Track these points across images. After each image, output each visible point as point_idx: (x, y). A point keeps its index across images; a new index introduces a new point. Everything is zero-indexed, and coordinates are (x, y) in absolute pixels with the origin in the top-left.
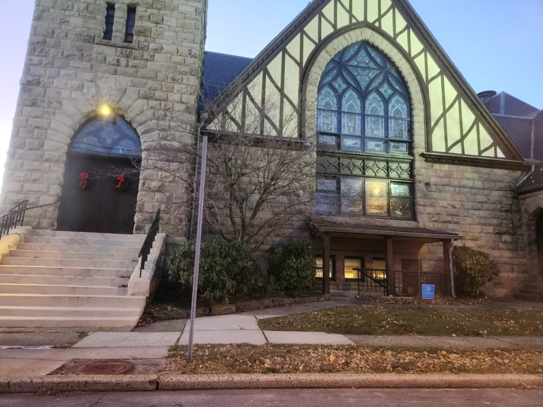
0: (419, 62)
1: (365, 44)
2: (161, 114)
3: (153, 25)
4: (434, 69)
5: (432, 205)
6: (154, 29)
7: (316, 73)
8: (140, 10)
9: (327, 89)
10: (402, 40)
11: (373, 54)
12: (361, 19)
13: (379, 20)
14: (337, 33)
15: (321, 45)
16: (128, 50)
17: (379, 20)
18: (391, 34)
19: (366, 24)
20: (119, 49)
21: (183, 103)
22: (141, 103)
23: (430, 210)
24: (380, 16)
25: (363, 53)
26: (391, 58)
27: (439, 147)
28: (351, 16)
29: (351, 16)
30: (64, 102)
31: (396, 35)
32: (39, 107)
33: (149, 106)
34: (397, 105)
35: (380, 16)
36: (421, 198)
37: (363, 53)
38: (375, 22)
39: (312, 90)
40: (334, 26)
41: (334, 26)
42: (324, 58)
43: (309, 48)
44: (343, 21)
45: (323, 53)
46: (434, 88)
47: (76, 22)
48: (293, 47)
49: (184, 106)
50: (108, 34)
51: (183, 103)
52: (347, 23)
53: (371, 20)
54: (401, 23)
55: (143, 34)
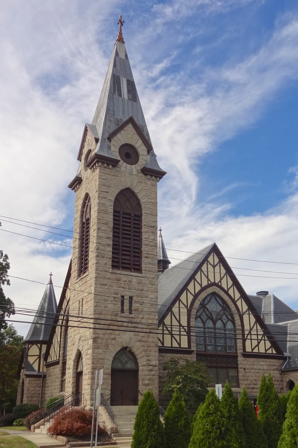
0: (239, 303)
1: (214, 294)
2: (146, 349)
3: (140, 305)
4: (245, 307)
5: (247, 380)
6: (140, 308)
7: (194, 312)
8: (134, 298)
9: (199, 319)
10: (231, 292)
11: (218, 299)
12: (213, 281)
13: (220, 281)
14: (203, 289)
15: (196, 296)
16: (132, 319)
17: (220, 281)
18: (226, 289)
19: (214, 284)
20: (128, 318)
21: (154, 342)
22: (138, 344)
23: (246, 382)
24: (221, 279)
25: (213, 300)
26: (224, 300)
27: (248, 349)
28: (208, 280)
29: (208, 280)
30: (110, 346)
31: (228, 289)
32: (100, 349)
33: (142, 345)
34: (229, 325)
35: (221, 279)
36: (242, 376)
37: (213, 300)
38: (219, 282)
39: (192, 320)
40: (201, 285)
41: (201, 285)
42: (197, 303)
43: (190, 298)
44: (205, 283)
45: (197, 301)
46: (246, 317)
47: (110, 306)
48: (183, 298)
49: (155, 344)
50: (122, 311)
51: (154, 342)
52: (207, 284)
53: (217, 282)
54: (230, 283)
55: (137, 310)
